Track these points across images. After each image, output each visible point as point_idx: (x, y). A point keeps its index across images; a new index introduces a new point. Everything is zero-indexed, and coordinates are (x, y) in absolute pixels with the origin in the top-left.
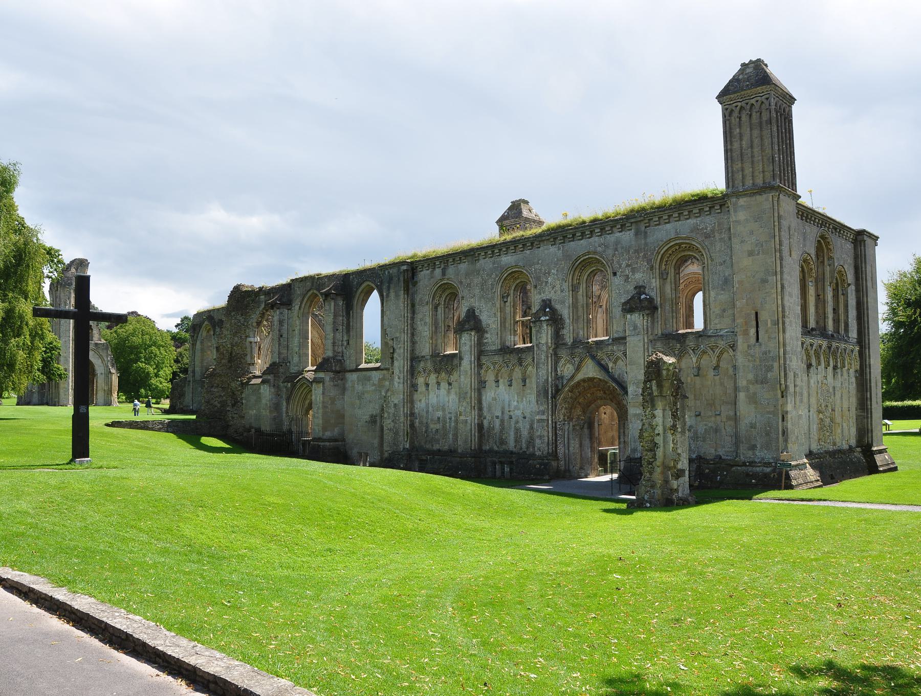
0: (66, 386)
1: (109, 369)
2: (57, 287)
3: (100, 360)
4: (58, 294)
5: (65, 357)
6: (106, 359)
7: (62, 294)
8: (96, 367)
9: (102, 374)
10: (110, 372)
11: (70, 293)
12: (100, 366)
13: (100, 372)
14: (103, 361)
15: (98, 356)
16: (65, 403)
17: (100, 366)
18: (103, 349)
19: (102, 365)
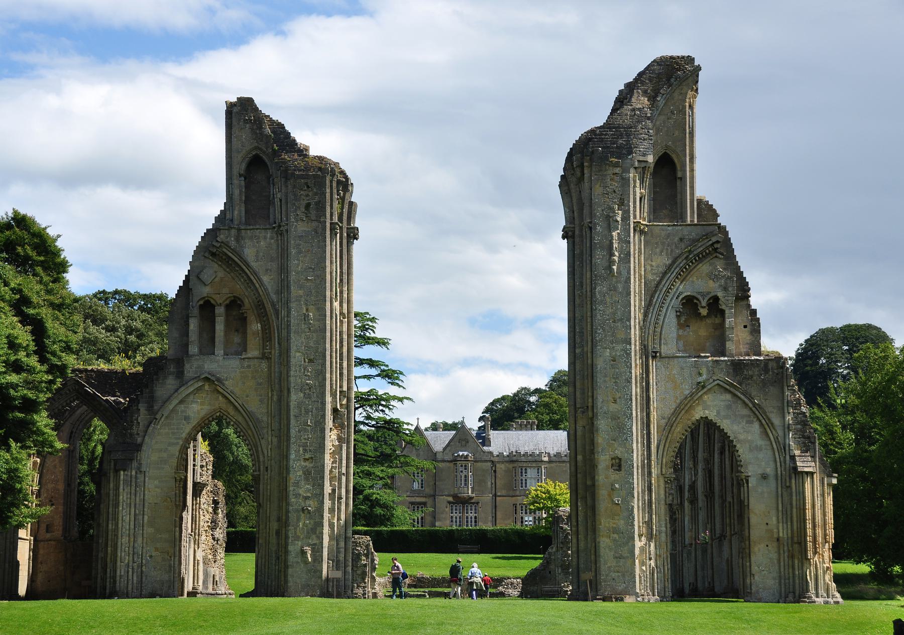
0: (622, 523)
1: (793, 458)
2: (582, 166)
3: (756, 425)
4: (586, 194)
5: (615, 418)
6: (776, 421)
7: (598, 190)
8: (742, 451)
9: (764, 477)
10: (795, 468)
11: (625, 182)
12: (759, 449)
13: (760, 471)
14: (766, 426)
15: (745, 412)
16: (621, 587)
17: (759, 449)
18: (764, 384)
19: (760, 442)
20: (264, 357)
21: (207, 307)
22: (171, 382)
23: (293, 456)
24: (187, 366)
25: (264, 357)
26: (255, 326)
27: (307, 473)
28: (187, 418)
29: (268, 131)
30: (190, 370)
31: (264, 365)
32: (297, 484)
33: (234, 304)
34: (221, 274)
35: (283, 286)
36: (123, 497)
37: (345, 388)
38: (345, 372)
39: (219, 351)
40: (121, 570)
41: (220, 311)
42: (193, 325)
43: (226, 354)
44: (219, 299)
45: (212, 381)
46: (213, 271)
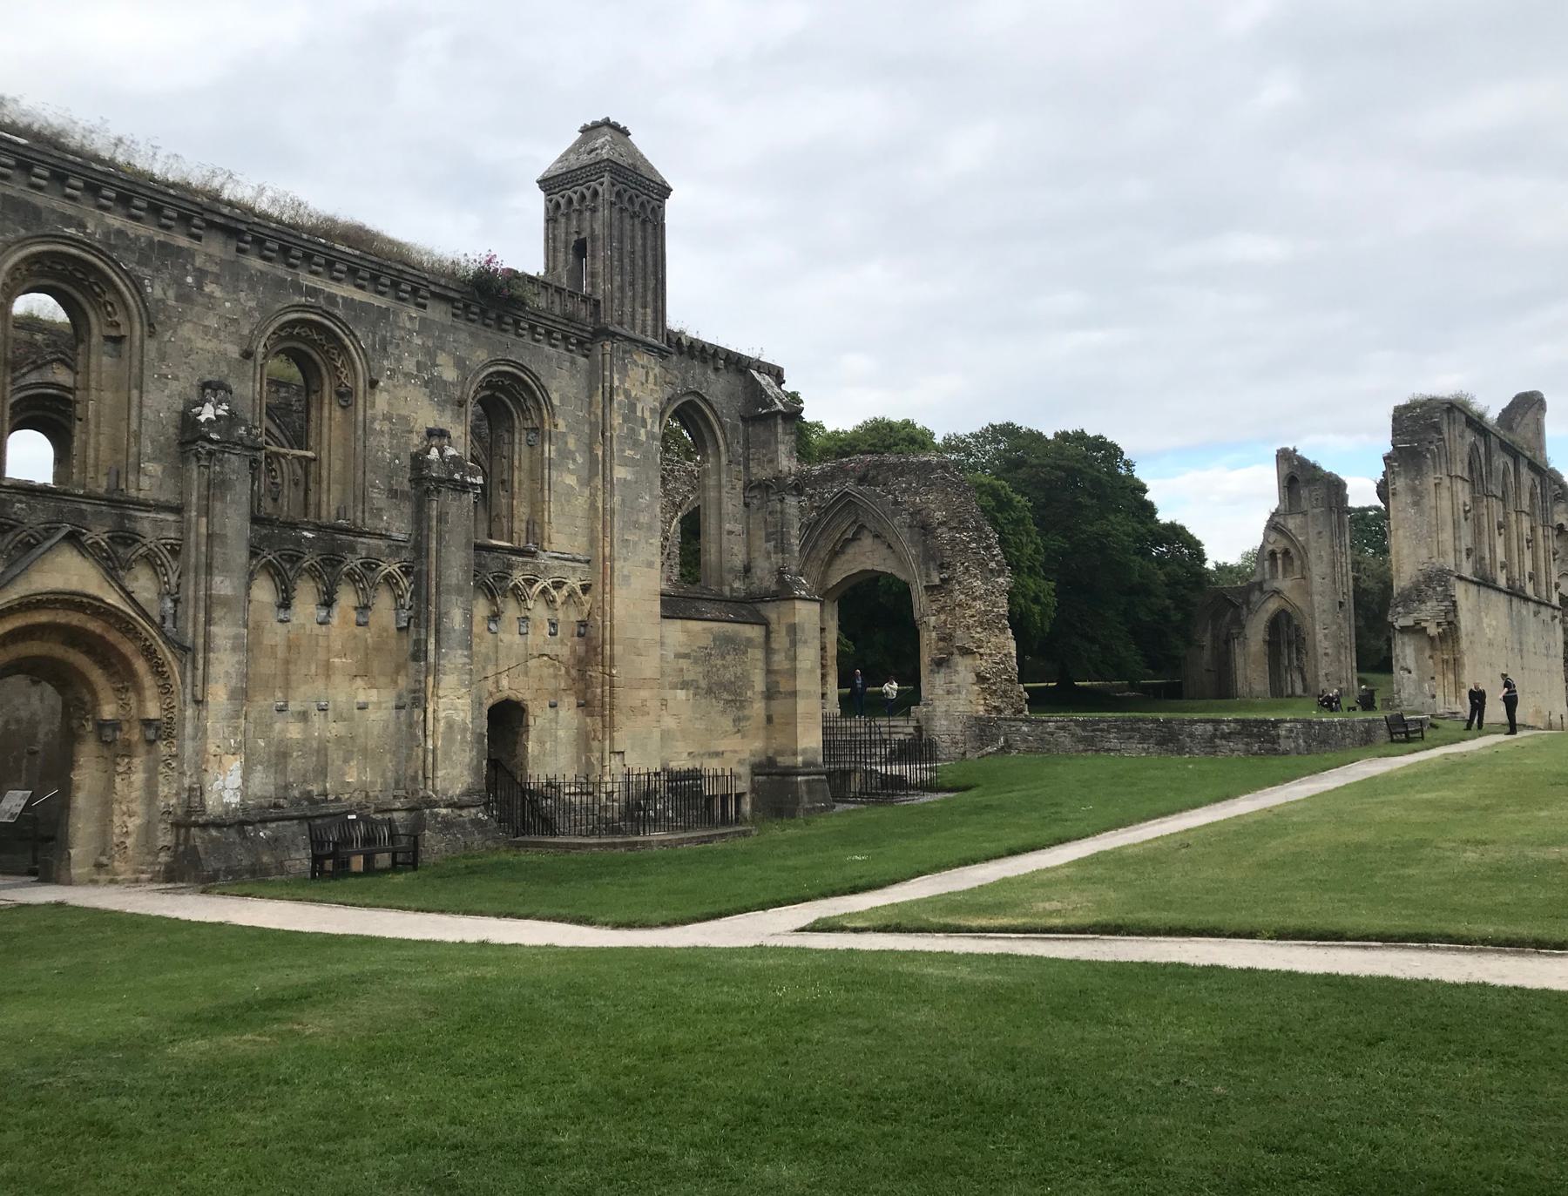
20: (1304, 578)
21: (1273, 554)
22: (1257, 593)
23: (1317, 627)
24: (1265, 586)
25: (1304, 578)
26: (1297, 563)
27: (1326, 636)
28: (1267, 611)
29: (1296, 463)
30: (1266, 587)
31: (1303, 582)
32: (1320, 641)
33: (1286, 553)
34: (1279, 537)
35: (1307, 540)
36: (1237, 651)
37: (1345, 590)
38: (1345, 582)
39: (1280, 576)
40: (1239, 685)
41: (1279, 556)
42: (1267, 564)
43: (1285, 576)
44: (1278, 550)
45: (1277, 592)
46: (1273, 536)
